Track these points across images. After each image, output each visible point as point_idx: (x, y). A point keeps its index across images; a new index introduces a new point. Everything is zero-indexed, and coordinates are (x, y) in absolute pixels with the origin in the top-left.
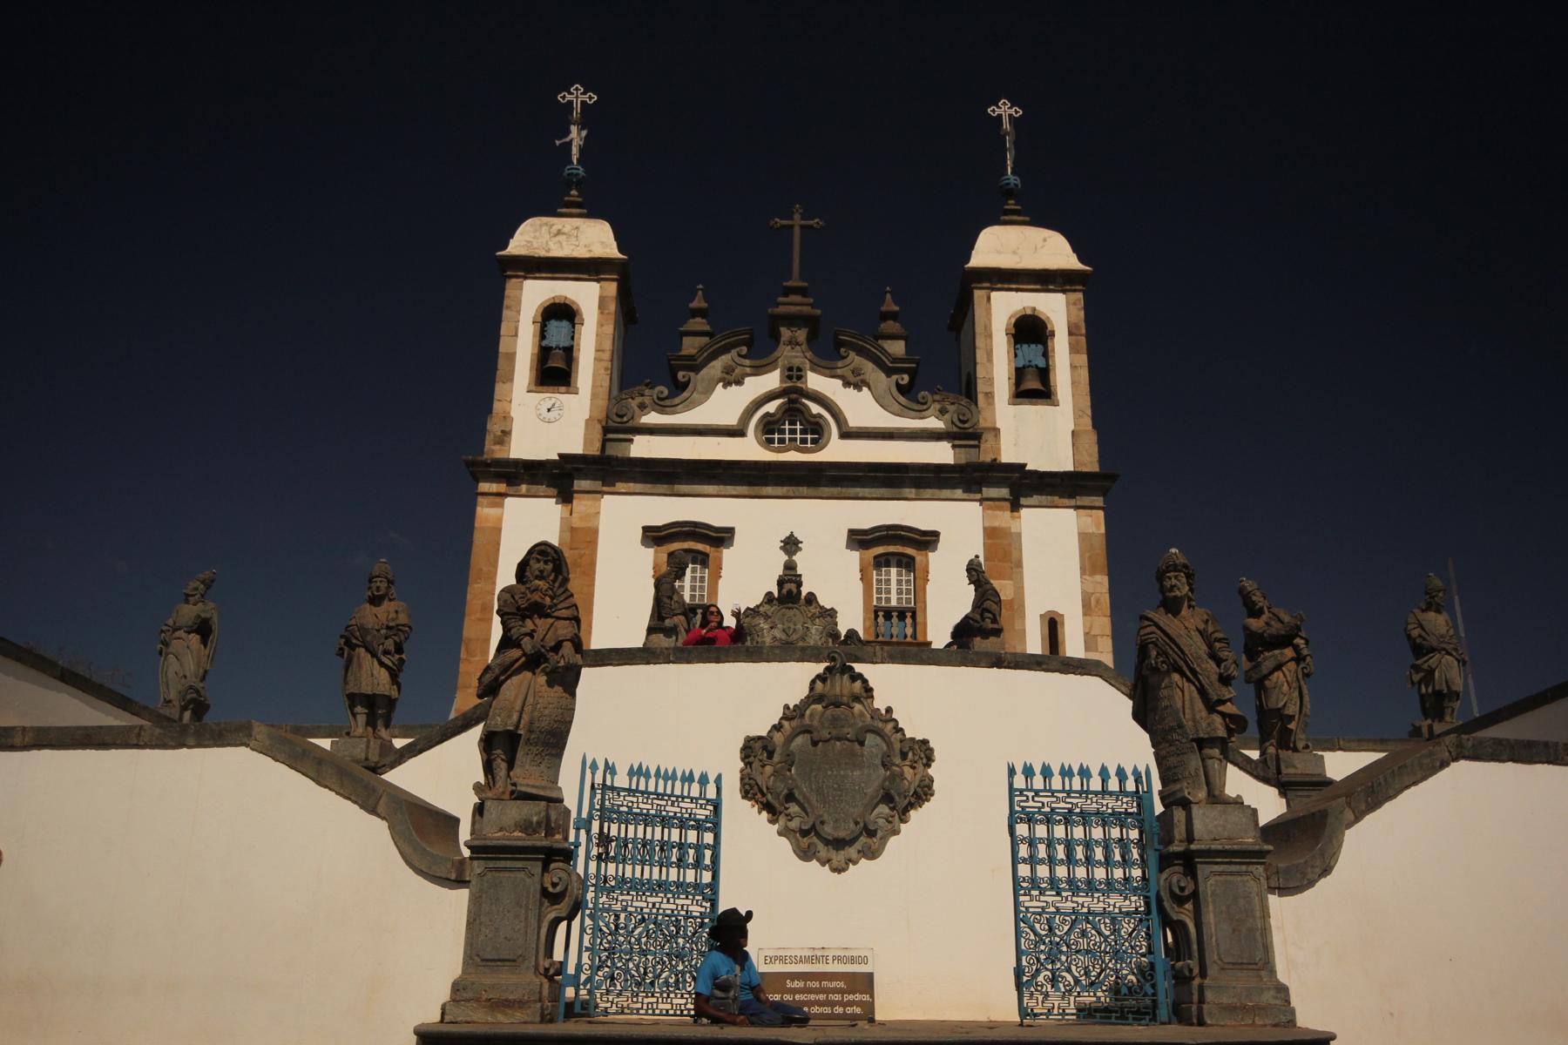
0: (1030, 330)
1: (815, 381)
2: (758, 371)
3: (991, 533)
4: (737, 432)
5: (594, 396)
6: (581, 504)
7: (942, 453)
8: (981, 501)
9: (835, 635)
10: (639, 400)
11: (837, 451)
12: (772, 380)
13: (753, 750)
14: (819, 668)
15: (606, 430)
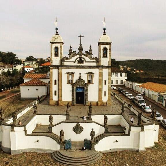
0: (105, 49)
1: (83, 56)
2: (77, 55)
3: (100, 73)
4: (75, 62)
5: (60, 58)
6: (60, 70)
7: (95, 64)
8: (99, 69)
9: (85, 83)
10: (65, 59)
11: (85, 64)
12: (78, 56)
13: (73, 128)
14: (77, 123)
15: (62, 62)
